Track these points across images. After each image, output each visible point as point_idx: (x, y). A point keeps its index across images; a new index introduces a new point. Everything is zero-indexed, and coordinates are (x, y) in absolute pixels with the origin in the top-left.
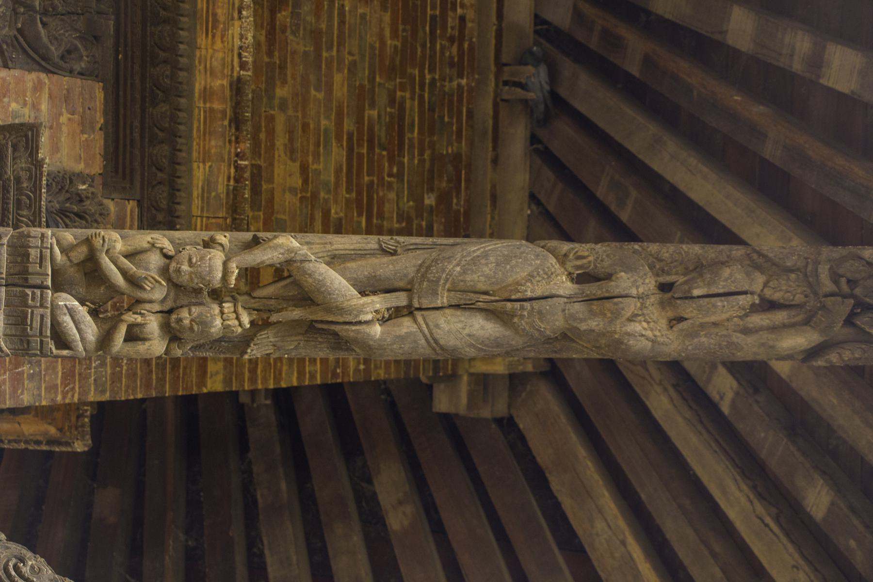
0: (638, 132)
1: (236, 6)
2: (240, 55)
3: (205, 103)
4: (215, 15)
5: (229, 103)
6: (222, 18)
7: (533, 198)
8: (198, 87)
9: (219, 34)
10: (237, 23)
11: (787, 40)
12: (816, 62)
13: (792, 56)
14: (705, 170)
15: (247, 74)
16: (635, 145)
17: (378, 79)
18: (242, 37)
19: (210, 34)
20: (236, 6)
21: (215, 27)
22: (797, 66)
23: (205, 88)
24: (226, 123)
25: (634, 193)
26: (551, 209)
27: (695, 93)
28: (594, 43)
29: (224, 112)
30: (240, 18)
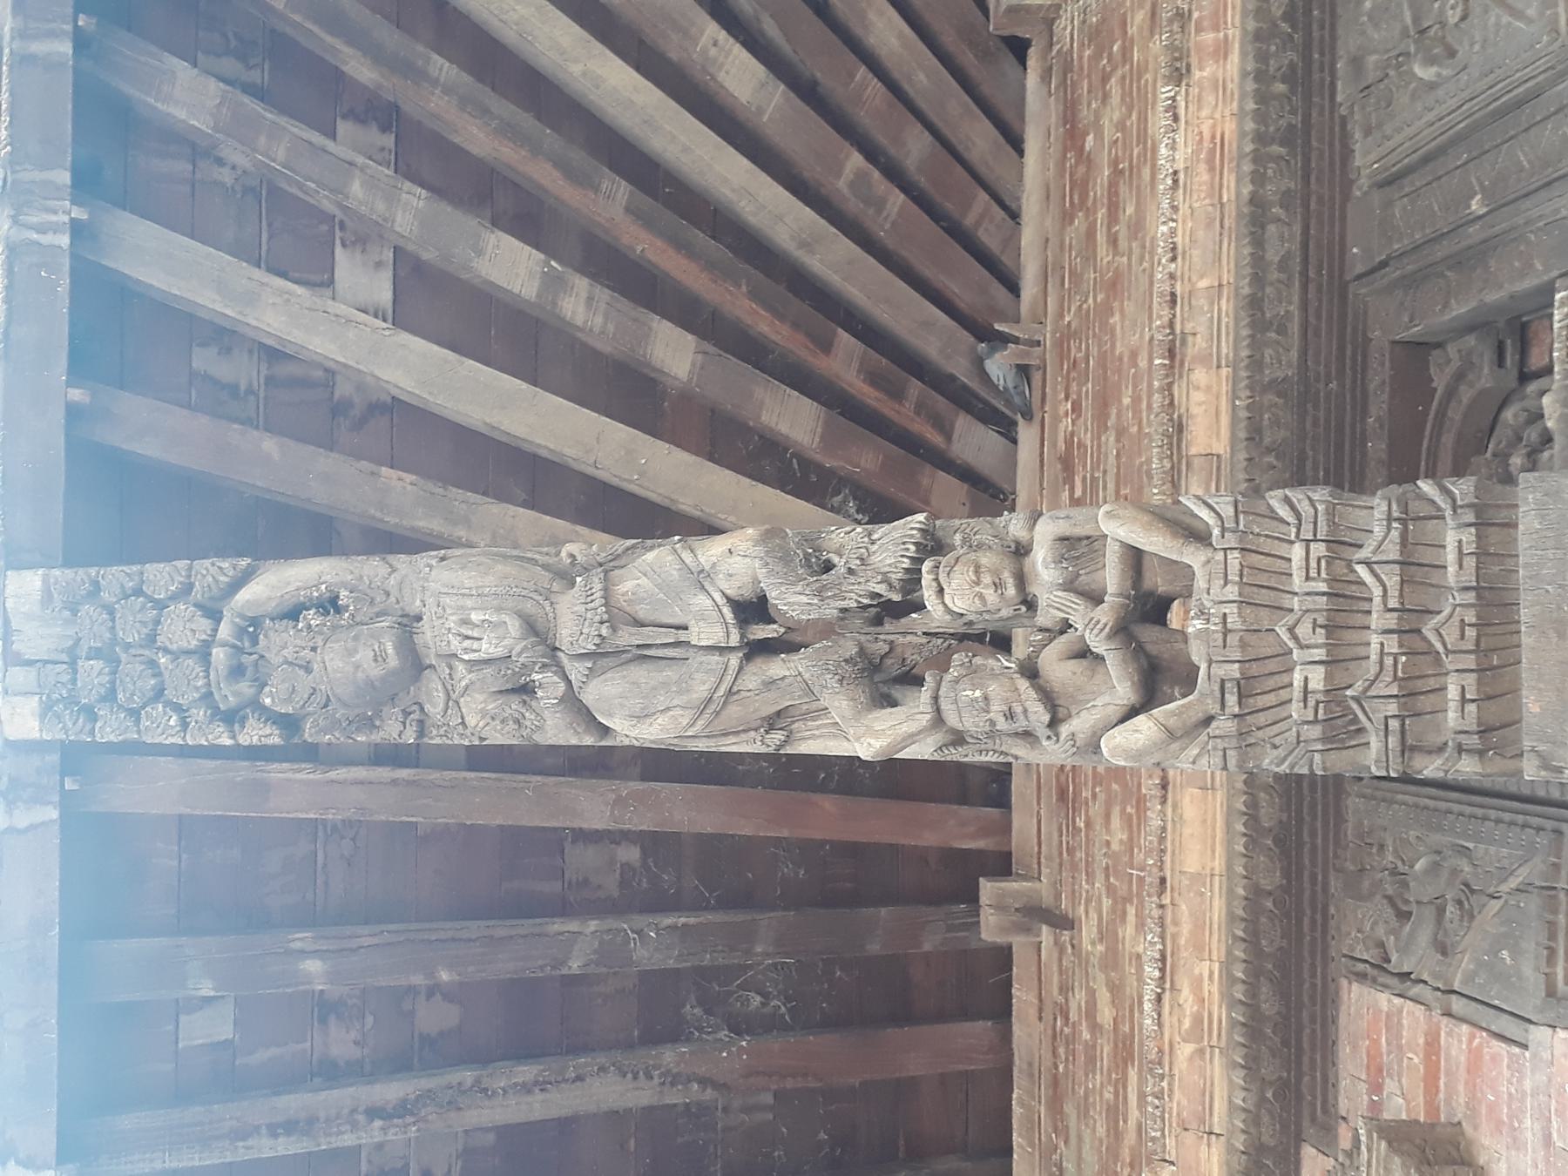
0: (833, 259)
1: (1181, 191)
2: (1176, 118)
3: (1226, 36)
4: (1211, 169)
5: (1192, 45)
6: (1202, 167)
7: (1015, 216)
8: (1235, 57)
9: (1206, 144)
10: (1180, 166)
11: (599, 320)
12: (552, 283)
13: (590, 299)
14: (728, 192)
15: (1165, 91)
16: (846, 247)
17: (1125, 259)
18: (1173, 147)
19: (1218, 141)
20: (1181, 191)
21: (1212, 152)
22: (582, 284)
23: (1225, 58)
24: (1196, 15)
25: (842, 184)
26: (983, 196)
27: (744, 288)
28: (915, 388)
29: (1199, 30)
30: (1175, 173)
